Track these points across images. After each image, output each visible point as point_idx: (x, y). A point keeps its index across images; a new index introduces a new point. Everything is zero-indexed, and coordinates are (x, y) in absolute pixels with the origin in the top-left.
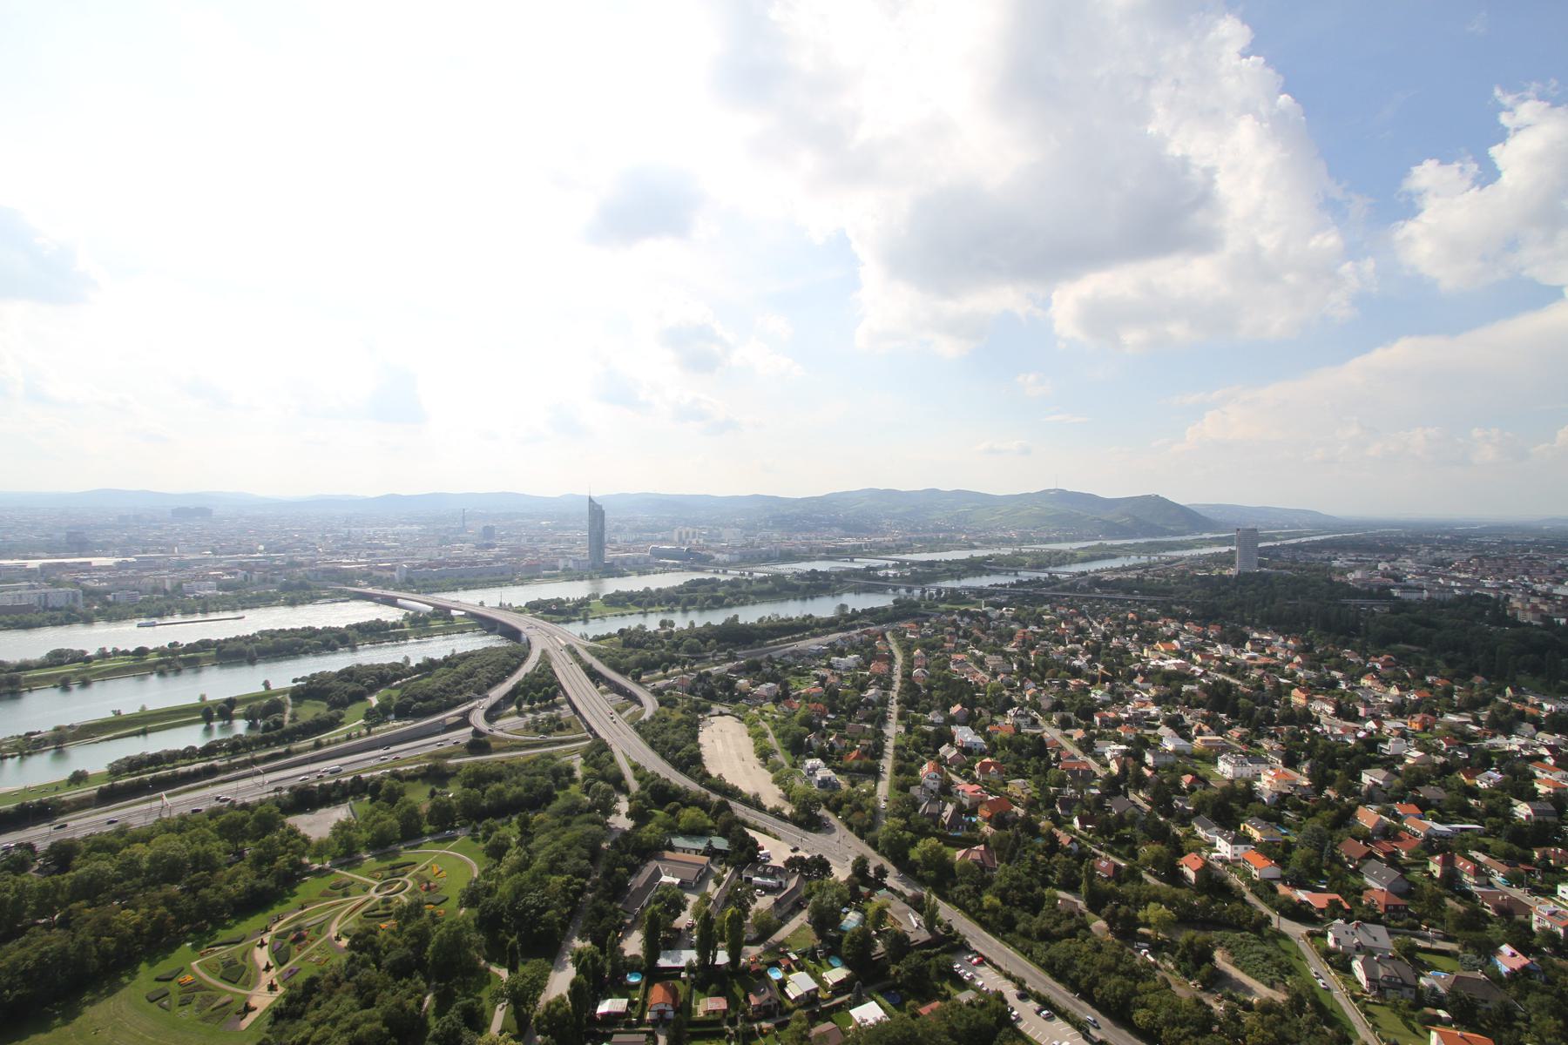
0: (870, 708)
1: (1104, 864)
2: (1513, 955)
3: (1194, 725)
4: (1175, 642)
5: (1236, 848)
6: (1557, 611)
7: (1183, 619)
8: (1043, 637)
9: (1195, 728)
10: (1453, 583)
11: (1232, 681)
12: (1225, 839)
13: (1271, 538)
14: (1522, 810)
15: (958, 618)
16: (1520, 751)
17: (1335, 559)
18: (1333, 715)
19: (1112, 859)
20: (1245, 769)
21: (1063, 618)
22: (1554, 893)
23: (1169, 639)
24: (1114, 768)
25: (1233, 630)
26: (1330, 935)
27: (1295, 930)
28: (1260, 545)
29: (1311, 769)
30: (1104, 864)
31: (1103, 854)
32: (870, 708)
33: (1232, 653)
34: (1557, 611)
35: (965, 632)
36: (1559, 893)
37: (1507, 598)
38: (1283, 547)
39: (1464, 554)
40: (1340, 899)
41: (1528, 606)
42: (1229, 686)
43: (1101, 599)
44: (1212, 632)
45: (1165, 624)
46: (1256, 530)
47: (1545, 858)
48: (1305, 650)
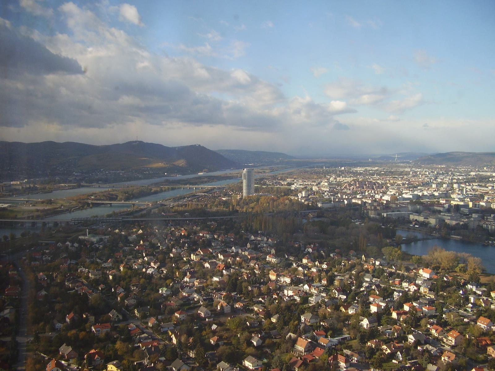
33: (240, 251)
39: (349, 179)
41: (373, 208)
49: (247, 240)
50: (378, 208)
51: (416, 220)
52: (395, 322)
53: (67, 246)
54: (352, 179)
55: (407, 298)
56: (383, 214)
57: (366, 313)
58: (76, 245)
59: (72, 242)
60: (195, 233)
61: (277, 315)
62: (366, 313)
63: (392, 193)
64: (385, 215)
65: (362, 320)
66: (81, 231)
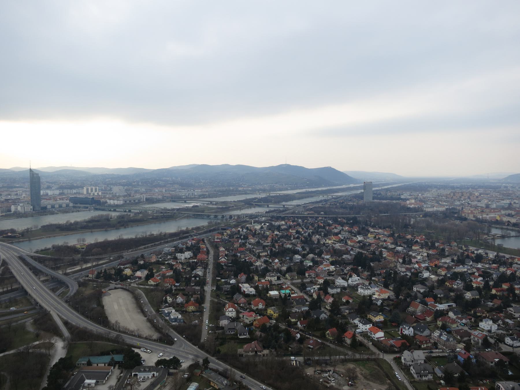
0: (198, 279)
1: (311, 342)
2: (465, 353)
3: (348, 273)
4: (339, 235)
5: (366, 326)
6: (479, 213)
7: (342, 224)
8: (282, 237)
9: (349, 274)
10: (444, 203)
11: (363, 252)
12: (362, 323)
13: (378, 186)
14: (468, 295)
15: (241, 230)
16: (467, 271)
17: (402, 195)
18: (402, 263)
19: (315, 338)
20: (369, 290)
21: (290, 227)
22: (478, 326)
23: (336, 234)
24: (315, 296)
25: (363, 229)
26: (402, 358)
27: (389, 358)
28: (374, 189)
29: (394, 288)
30: (311, 342)
31: (311, 337)
32: (198, 279)
34: (479, 213)
35: (244, 236)
36: (480, 326)
37: (462, 209)
38: (382, 190)
40: (406, 342)
41: (470, 212)
42: (361, 253)
43: (307, 217)
44: (356, 229)
45: (336, 228)
46: (371, 182)
47: (475, 313)
48: (392, 235)
49: (369, 231)
50: (475, 212)
51: (509, 221)
52: (494, 297)
53: (239, 231)
54: (450, 191)
55: (503, 278)
56: (478, 217)
57: (469, 287)
58: (245, 230)
59: (242, 228)
60: (329, 225)
61: (392, 285)
62: (469, 287)
63: (486, 201)
64: (481, 217)
65: (466, 293)
66: (248, 221)
